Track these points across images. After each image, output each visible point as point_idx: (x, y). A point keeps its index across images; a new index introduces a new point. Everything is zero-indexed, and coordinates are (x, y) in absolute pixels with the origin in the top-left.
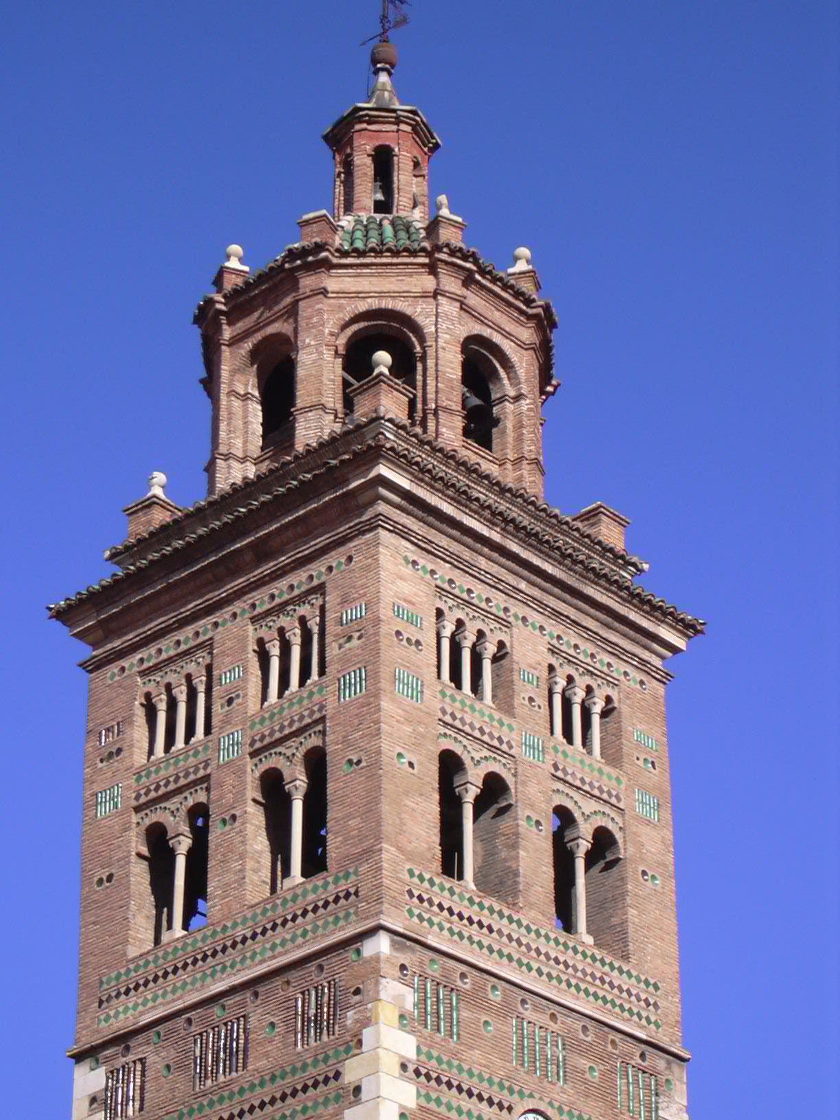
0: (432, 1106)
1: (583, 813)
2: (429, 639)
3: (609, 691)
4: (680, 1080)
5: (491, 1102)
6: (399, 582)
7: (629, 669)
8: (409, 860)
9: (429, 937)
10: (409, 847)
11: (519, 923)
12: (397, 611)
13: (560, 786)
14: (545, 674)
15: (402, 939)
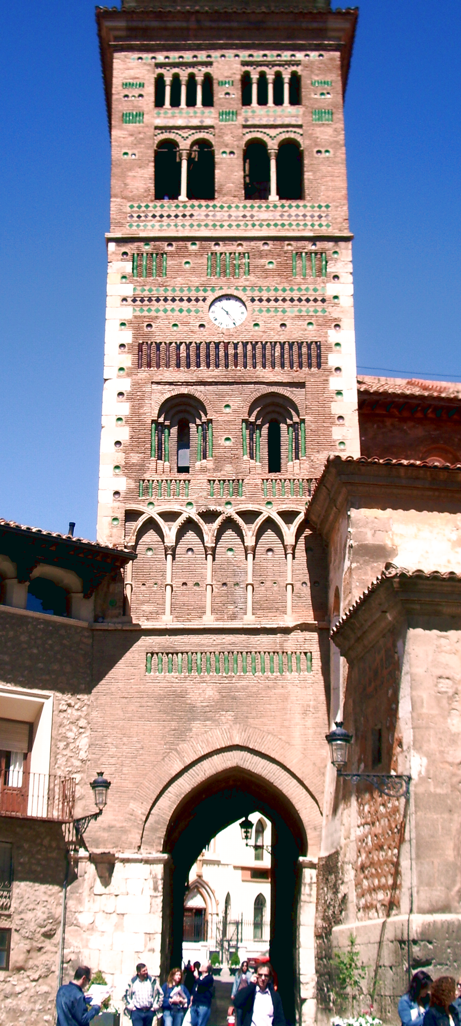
0: (146, 313)
1: (271, 137)
2: (150, 90)
3: (294, 68)
4: (347, 249)
5: (189, 300)
6: (127, 72)
7: (308, 53)
8: (130, 201)
9: (141, 233)
10: (130, 195)
11: (214, 206)
12: (126, 85)
13: (248, 130)
14: (238, 77)
15: (120, 241)
